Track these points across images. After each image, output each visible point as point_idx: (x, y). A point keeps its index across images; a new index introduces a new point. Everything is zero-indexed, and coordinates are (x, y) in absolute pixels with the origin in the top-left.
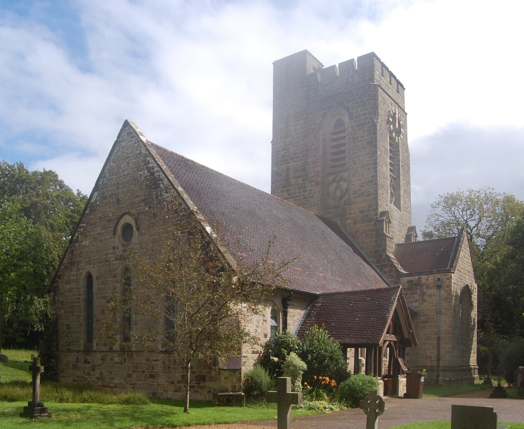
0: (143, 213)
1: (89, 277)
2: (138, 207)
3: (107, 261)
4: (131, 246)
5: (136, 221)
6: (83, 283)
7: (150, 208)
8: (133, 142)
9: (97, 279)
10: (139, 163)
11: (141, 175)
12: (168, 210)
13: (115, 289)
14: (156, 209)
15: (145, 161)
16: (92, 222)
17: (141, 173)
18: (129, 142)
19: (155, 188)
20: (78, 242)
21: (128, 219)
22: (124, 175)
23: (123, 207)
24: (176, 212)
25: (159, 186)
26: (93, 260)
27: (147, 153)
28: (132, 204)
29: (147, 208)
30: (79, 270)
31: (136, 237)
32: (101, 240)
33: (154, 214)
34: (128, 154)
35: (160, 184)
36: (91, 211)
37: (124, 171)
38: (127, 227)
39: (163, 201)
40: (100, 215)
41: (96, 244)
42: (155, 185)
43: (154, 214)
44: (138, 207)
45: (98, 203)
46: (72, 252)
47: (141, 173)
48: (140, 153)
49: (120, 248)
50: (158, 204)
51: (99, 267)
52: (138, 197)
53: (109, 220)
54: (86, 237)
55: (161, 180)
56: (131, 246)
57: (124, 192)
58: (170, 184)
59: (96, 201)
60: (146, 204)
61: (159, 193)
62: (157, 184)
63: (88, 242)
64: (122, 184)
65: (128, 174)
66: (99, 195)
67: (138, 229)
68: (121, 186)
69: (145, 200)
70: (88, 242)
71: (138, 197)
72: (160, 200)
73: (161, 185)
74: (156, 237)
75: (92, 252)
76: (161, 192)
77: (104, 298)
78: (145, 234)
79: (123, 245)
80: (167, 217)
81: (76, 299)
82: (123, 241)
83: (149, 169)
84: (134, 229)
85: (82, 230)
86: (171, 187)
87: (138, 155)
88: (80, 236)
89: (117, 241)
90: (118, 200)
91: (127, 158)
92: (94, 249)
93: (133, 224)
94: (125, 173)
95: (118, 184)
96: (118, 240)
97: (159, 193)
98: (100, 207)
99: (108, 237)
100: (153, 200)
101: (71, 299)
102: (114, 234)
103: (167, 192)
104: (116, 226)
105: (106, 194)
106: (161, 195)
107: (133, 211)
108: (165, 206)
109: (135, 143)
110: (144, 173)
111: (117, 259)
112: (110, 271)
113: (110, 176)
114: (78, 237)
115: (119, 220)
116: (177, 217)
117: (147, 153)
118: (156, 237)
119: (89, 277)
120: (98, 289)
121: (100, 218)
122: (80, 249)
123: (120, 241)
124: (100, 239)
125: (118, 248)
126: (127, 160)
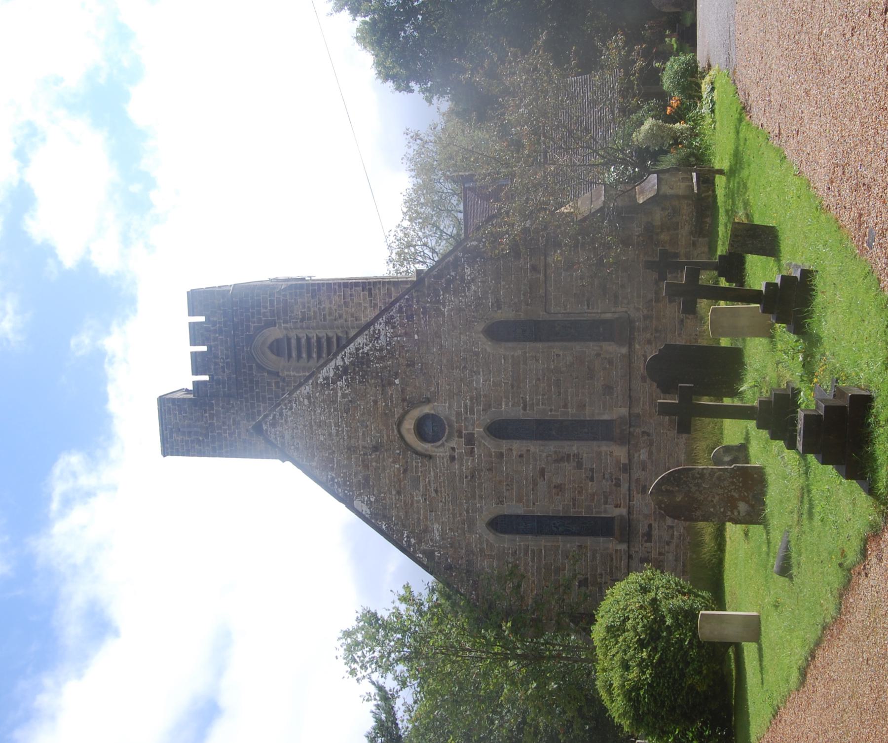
0: (403, 390)
2: (392, 402)
3: (472, 477)
4: (454, 418)
6: (508, 542)
7: (397, 375)
8: (289, 413)
9: (502, 502)
10: (324, 401)
11: (344, 396)
12: (406, 334)
13: (521, 456)
14: (401, 360)
15: (322, 385)
16: (401, 514)
17: (339, 394)
18: (286, 421)
19: (369, 361)
20: (433, 552)
21: (409, 425)
22: (337, 435)
23: (388, 436)
24: (410, 318)
25: (367, 354)
26: (468, 512)
27: (311, 381)
28: (386, 414)
29: (397, 381)
30: (482, 550)
31: (440, 408)
32: (436, 491)
33: (408, 365)
34: (305, 426)
35: (363, 353)
36: (384, 517)
37: (330, 434)
39: (391, 343)
40: (394, 493)
41: (441, 504)
42: (363, 364)
43: (408, 365)
44: (392, 402)
45: (372, 499)
46: (449, 568)
47: (339, 394)
48: (309, 398)
49: (453, 444)
50: (393, 357)
51: (481, 497)
52: (375, 402)
53: (405, 471)
54: (426, 530)
55: (357, 349)
56: (454, 418)
57: (363, 434)
58: (367, 332)
59: (369, 504)
60: (391, 383)
61: (378, 354)
62: (363, 358)
63: (436, 526)
64: (350, 437)
65: (337, 425)
66: (361, 494)
67: (428, 401)
68: (353, 441)
69: (383, 386)
70: (436, 526)
71: (375, 402)
72: (389, 352)
73: (366, 349)
74: (445, 361)
75: (454, 515)
76: (375, 349)
77: (535, 484)
78: (438, 384)
80: (416, 337)
81: (533, 561)
82: (444, 439)
83: (338, 377)
84: (426, 409)
85: (413, 541)
86: (372, 328)
87: (310, 402)
88: (423, 547)
89: (440, 451)
90: (376, 448)
91: (311, 427)
92: (449, 510)
93: (416, 413)
95: (349, 449)
96: (441, 449)
97: (378, 354)
98: (380, 493)
99: (432, 474)
100: (386, 367)
101: (533, 574)
102: (430, 457)
103: (378, 338)
104: (417, 453)
105: (360, 477)
106: (381, 350)
107: (398, 412)
108: (398, 342)
109: (291, 409)
110: (341, 388)
111: (472, 452)
112: (490, 470)
114: (424, 552)
115: (408, 447)
116: (419, 315)
117: (311, 381)
118: (445, 361)
120: (520, 500)
121: (399, 493)
122: (447, 547)
123: (443, 445)
124: (433, 494)
125: (453, 449)
126: (315, 428)
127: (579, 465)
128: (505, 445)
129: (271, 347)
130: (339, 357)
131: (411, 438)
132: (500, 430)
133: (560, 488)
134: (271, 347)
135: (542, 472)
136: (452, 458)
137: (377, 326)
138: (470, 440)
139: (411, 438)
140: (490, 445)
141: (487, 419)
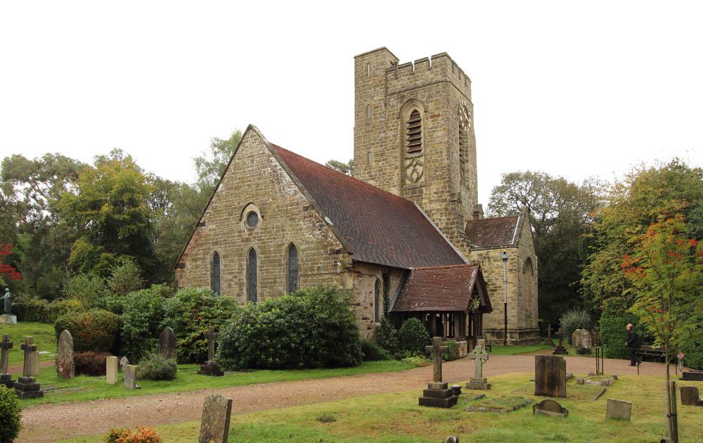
1: (216, 255)
5: (260, 209)
38: (252, 214)
48: (263, 153)
59: (222, 191)
67: (263, 217)
73: (284, 181)
79: (250, 230)
87: (261, 154)
94: (249, 169)
111: (243, 241)
113: (235, 170)
119: (216, 255)
127: (239, 295)
128: (246, 255)
129: (415, 111)
130: (280, 167)
131: (248, 210)
132: (252, 253)
133: (230, 286)
134: (415, 111)
135: (235, 277)
136: (240, 232)
137: (294, 186)
138: (248, 240)
139: (248, 210)
140: (247, 249)
141: (256, 247)
